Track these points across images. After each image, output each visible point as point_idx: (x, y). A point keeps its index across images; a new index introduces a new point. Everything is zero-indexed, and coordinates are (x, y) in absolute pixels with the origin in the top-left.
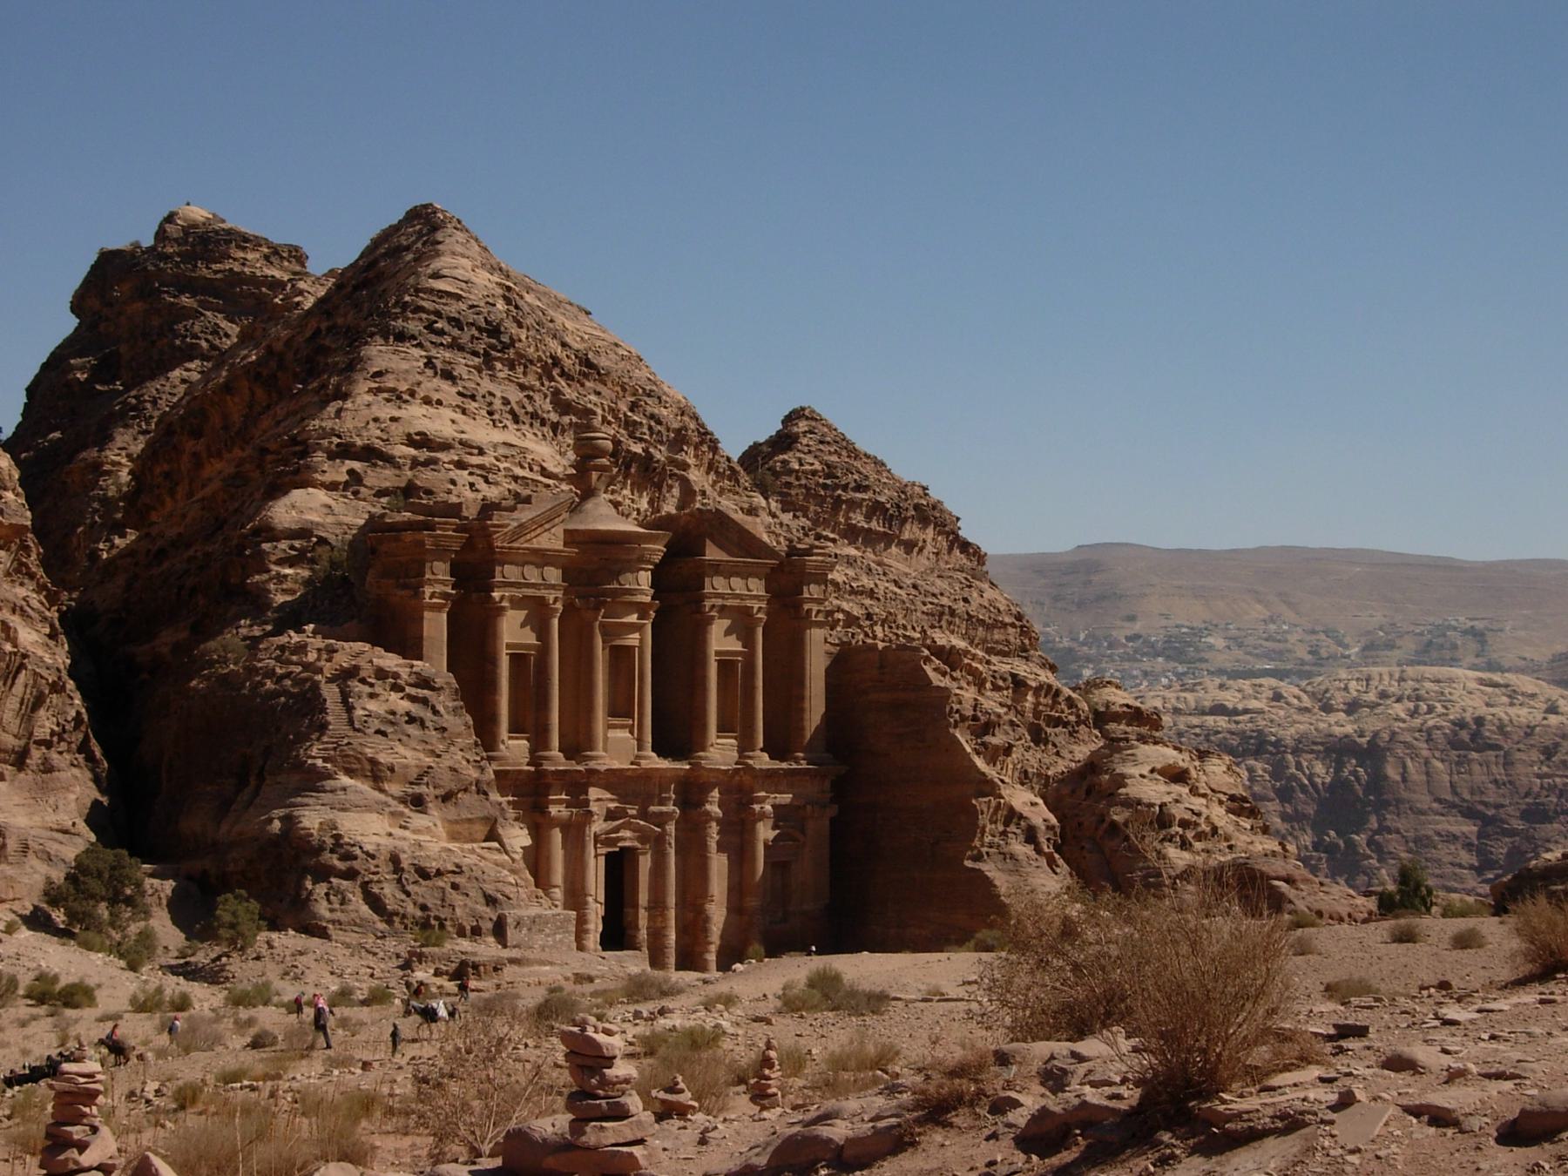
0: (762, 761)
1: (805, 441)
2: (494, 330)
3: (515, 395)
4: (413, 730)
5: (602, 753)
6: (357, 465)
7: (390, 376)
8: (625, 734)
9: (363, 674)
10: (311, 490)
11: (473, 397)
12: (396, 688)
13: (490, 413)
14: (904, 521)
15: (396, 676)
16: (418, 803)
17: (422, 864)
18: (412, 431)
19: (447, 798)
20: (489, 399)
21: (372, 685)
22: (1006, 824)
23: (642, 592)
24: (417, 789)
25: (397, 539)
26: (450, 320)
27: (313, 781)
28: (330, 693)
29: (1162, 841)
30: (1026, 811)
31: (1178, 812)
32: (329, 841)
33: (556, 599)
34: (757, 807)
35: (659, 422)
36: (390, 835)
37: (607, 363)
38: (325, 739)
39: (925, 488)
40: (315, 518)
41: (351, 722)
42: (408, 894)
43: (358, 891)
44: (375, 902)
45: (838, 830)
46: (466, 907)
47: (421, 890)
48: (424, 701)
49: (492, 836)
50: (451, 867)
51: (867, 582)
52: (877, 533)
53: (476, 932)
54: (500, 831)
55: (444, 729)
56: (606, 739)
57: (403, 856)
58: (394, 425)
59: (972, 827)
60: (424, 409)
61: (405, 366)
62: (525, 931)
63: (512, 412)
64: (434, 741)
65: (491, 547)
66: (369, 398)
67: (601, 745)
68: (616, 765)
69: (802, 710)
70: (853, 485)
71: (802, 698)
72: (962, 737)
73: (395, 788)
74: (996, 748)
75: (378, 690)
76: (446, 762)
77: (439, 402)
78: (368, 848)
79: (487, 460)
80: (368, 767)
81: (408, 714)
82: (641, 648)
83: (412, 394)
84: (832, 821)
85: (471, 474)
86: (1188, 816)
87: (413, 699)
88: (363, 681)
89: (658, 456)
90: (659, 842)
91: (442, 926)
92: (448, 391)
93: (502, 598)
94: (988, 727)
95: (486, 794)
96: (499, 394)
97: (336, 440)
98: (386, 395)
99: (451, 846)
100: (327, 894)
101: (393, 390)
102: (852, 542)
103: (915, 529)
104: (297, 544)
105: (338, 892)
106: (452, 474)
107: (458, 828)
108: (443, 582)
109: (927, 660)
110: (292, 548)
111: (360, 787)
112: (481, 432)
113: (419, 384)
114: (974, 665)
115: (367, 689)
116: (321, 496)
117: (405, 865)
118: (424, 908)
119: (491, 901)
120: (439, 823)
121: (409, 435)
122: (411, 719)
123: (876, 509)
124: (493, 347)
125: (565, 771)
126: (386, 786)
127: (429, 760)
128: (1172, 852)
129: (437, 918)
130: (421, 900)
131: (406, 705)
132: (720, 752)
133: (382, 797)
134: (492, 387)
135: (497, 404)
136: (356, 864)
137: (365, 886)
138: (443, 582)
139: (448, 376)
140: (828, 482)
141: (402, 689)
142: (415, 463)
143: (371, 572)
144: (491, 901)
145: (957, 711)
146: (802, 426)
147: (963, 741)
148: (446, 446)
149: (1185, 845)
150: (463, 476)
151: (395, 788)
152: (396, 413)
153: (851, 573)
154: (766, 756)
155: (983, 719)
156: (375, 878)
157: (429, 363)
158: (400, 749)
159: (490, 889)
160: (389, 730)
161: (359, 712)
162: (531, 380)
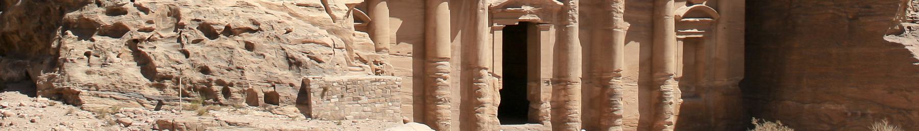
17: (208, 20)
42: (187, 54)
43: (128, 53)
44: (146, 65)
46: (257, 71)
47: (208, 52)
50: (243, 23)
53: (272, 99)
57: (183, 11)
62: (335, 99)
91: (227, 93)
100: (88, 54)
117: (186, 20)
118: (205, 70)
119: (294, 63)
129: (220, 82)
130: (201, 62)
136: (124, 19)
137: (133, 44)
144: (294, 63)
156: (147, 35)
159: (295, 51)
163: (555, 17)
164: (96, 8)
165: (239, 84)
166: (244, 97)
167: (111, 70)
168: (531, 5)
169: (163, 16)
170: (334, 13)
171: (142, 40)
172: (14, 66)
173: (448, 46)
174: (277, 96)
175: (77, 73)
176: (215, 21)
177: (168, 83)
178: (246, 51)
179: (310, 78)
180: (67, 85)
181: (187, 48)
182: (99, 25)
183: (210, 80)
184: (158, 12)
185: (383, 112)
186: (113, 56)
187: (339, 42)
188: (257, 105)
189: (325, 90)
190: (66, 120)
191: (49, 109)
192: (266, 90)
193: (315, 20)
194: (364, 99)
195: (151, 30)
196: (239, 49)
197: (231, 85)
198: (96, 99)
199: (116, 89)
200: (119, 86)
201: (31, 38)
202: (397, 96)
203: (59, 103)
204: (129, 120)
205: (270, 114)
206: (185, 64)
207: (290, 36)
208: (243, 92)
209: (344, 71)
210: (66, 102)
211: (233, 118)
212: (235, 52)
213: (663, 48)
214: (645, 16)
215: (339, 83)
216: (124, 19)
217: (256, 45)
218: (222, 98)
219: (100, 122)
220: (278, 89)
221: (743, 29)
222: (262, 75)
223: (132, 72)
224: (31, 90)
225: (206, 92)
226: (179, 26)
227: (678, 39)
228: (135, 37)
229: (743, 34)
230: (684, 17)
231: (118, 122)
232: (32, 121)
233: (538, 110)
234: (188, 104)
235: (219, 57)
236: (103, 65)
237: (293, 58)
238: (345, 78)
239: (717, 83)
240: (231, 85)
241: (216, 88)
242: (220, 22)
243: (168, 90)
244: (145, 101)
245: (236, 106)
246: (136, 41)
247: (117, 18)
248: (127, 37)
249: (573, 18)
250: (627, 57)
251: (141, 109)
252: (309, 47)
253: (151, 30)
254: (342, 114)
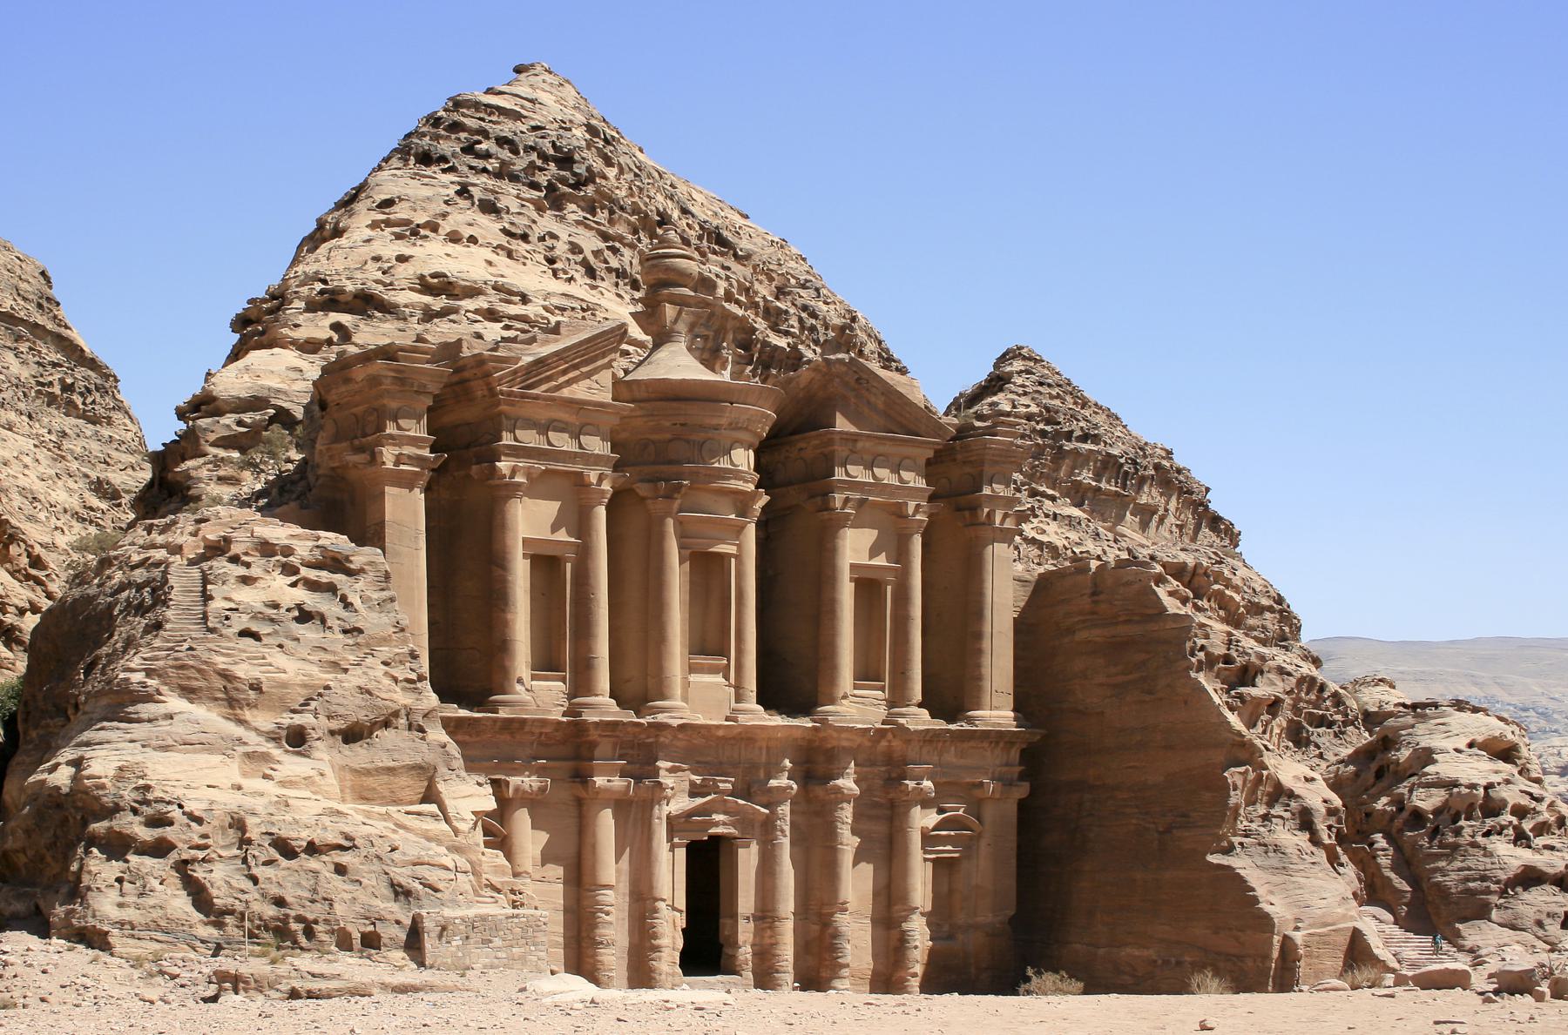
0: (919, 719)
1: (1019, 381)
2: (565, 160)
3: (590, 243)
4: (308, 632)
5: (679, 703)
6: (346, 319)
7: (404, 205)
8: (719, 679)
9: (236, 549)
10: (276, 350)
11: (525, 238)
12: (289, 570)
13: (551, 261)
14: (1142, 481)
15: (288, 551)
16: (297, 739)
17: (284, 833)
18: (426, 273)
19: (352, 735)
20: (549, 242)
21: (248, 565)
22: (1270, 805)
23: (737, 474)
24: (298, 720)
25: (348, 380)
26: (502, 141)
27: (121, 704)
28: (182, 579)
29: (1487, 834)
30: (1299, 788)
31: (1511, 796)
32: (129, 796)
33: (601, 479)
34: (911, 784)
35: (813, 315)
36: (239, 788)
37: (749, 246)
38: (157, 643)
39: (1169, 453)
40: (274, 383)
41: (205, 617)
42: (255, 880)
43: (174, 879)
44: (199, 895)
45: (1029, 816)
46: (350, 903)
47: (283, 877)
48: (331, 588)
49: (430, 795)
50: (333, 838)
52: (1108, 493)
53: (371, 942)
54: (441, 787)
55: (360, 631)
56: (687, 684)
57: (251, 821)
58: (404, 265)
59: (1222, 814)
60: (452, 248)
61: (426, 192)
62: (457, 942)
63: (585, 263)
64: (339, 648)
65: (492, 393)
66: (368, 233)
67: (678, 691)
68: (701, 720)
69: (980, 652)
70: (1078, 433)
71: (979, 636)
72: (1210, 684)
73: (264, 720)
74: (1258, 701)
75: (255, 571)
76: (355, 679)
77: (473, 240)
78: (190, 806)
79: (531, 310)
80: (219, 683)
81: (299, 607)
82: (739, 558)
83: (434, 228)
84: (1022, 805)
85: (507, 328)
86: (1525, 801)
87: (313, 586)
88: (235, 560)
89: (809, 354)
90: (766, 832)
91: (309, 933)
92: (489, 228)
93: (514, 471)
94: (1247, 675)
95: (421, 730)
96: (564, 236)
97: (319, 286)
98: (397, 230)
99: (342, 808)
100: (120, 880)
101: (406, 223)
102: (1079, 505)
103: (1154, 492)
104: (247, 418)
105: (136, 876)
106: (478, 327)
107: (370, 781)
108: (414, 441)
109: (1160, 580)
110: (240, 423)
111: (208, 716)
112: (530, 277)
113: (444, 215)
114: (1228, 592)
115: (242, 571)
116: (290, 357)
117: (253, 833)
118: (280, 902)
119: (401, 892)
120: (328, 770)
121: (422, 277)
122: (304, 616)
123: (1108, 465)
124: (563, 181)
125: (615, 724)
126: (247, 714)
127: (328, 677)
128: (1502, 847)
129: (300, 919)
130: (274, 890)
131: (301, 595)
132: (855, 708)
133: (239, 731)
134: (556, 228)
135: (561, 249)
136: (169, 833)
137: (182, 867)
138: (414, 441)
139: (489, 208)
140: (1048, 428)
141: (295, 571)
143: (322, 434)
144: (401, 892)
145: (1202, 648)
146: (1018, 365)
147: (1210, 689)
148: (473, 292)
149: (1520, 838)
151: (264, 720)
152: (407, 251)
153: (1074, 536)
154: (925, 713)
155: (1240, 661)
156: (200, 854)
157: (464, 191)
158: (279, 659)
159: (402, 876)
160: (263, 629)
161: (217, 605)
162: (621, 229)
163: (757, 830)
164: (131, 817)
165: (326, 921)
166: (334, 939)
167: (151, 901)
168: (725, 813)
169: (222, 828)
170: (455, 823)
171: (194, 860)
172: (19, 897)
173: (611, 869)
174: (379, 937)
175: (106, 906)
176: (293, 834)
177: (229, 919)
178: (336, 876)
179: (424, 912)
180: (91, 922)
181: (255, 871)
182: (135, 840)
183: (287, 916)
184: (215, 823)
185: (523, 959)
186: (155, 883)
187: (462, 863)
188: (351, 950)
189: (444, 928)
190: (90, 970)
191: (68, 955)
192: (363, 929)
193: (431, 834)
194: (497, 942)
195: (206, 847)
196: (327, 873)
197: (316, 922)
198: (130, 941)
199: (159, 928)
200: (163, 923)
201: (42, 859)
202: (542, 938)
203: (80, 947)
204: (176, 971)
205: (368, 962)
206: (253, 894)
207: (396, 855)
208: (332, 932)
209: (470, 903)
210: (90, 946)
211: (318, 968)
212: (321, 877)
213: (905, 872)
214: (880, 828)
215: (462, 919)
216: (169, 833)
217: (350, 867)
218: (303, 940)
219: (136, 973)
220: (380, 928)
221: (1014, 845)
222: (358, 908)
223: (181, 904)
224: (43, 929)
225: (281, 932)
226: (244, 842)
227: (926, 860)
228: (185, 856)
229: (1014, 853)
230: (935, 828)
231: (162, 973)
232: (44, 972)
233: (734, 957)
234: (257, 948)
235: (299, 884)
236: (141, 895)
237: (400, 886)
238: (471, 912)
239: (980, 919)
240: (316, 922)
241: (295, 926)
242: (300, 836)
243: (229, 929)
244: (198, 944)
245: (322, 951)
246: (186, 862)
247: (160, 830)
248: (174, 856)
249: (782, 831)
250: (856, 884)
251: (192, 955)
252: (422, 871)
253: (206, 847)
254: (468, 962)
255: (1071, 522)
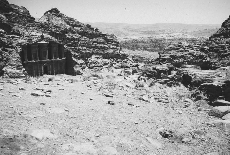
2: (42, 25)
6: (27, 37)
16: (14, 67)
51: (87, 40)
73: (13, 66)
76: (18, 64)
79: (37, 37)
92: (36, 31)
112: (38, 34)
119: (19, 75)
131: (16, 60)
139: (36, 29)
142: (31, 37)
148: (34, 36)
150: (35, 38)
157: (35, 28)
159: (18, 74)
255: (85, 38)
